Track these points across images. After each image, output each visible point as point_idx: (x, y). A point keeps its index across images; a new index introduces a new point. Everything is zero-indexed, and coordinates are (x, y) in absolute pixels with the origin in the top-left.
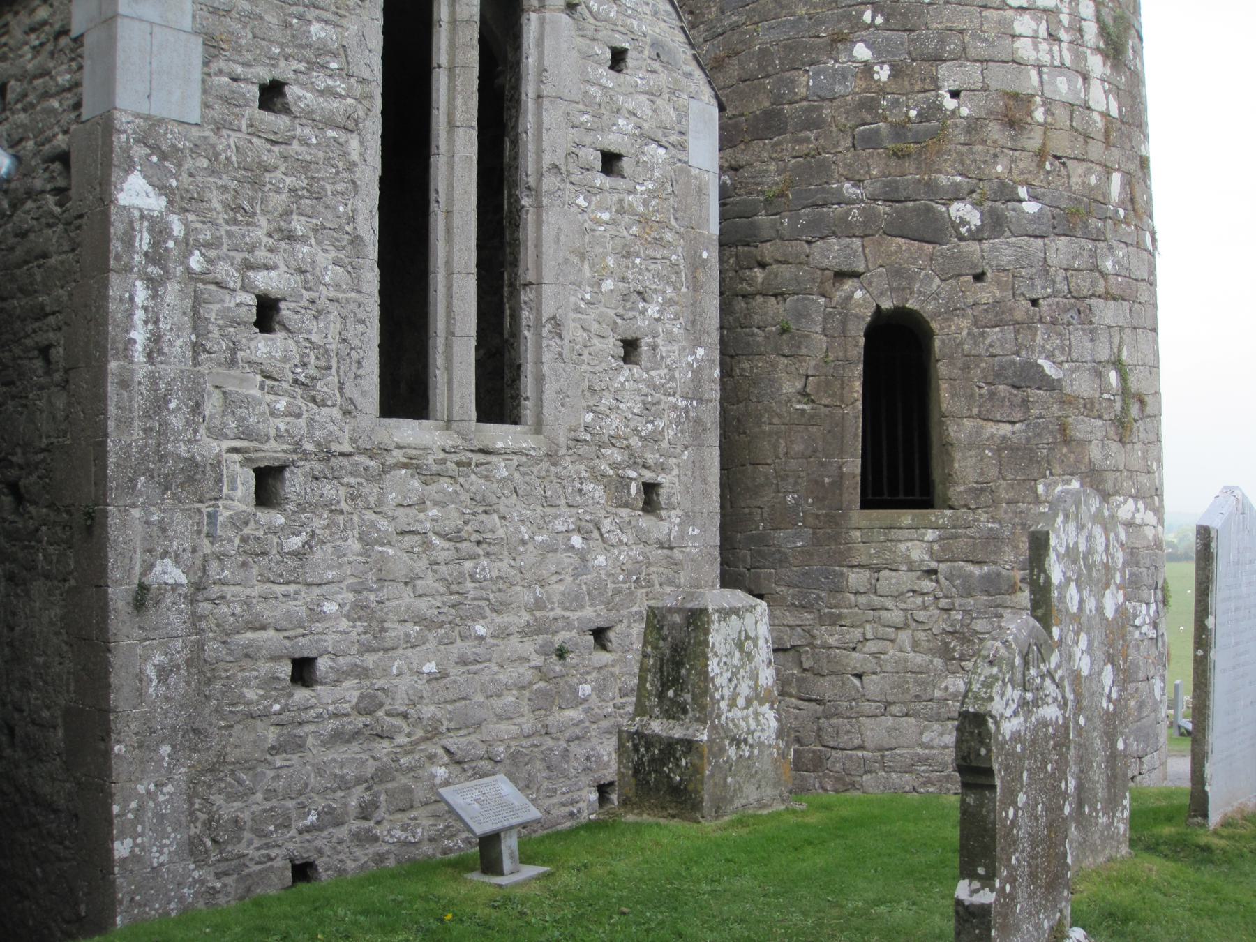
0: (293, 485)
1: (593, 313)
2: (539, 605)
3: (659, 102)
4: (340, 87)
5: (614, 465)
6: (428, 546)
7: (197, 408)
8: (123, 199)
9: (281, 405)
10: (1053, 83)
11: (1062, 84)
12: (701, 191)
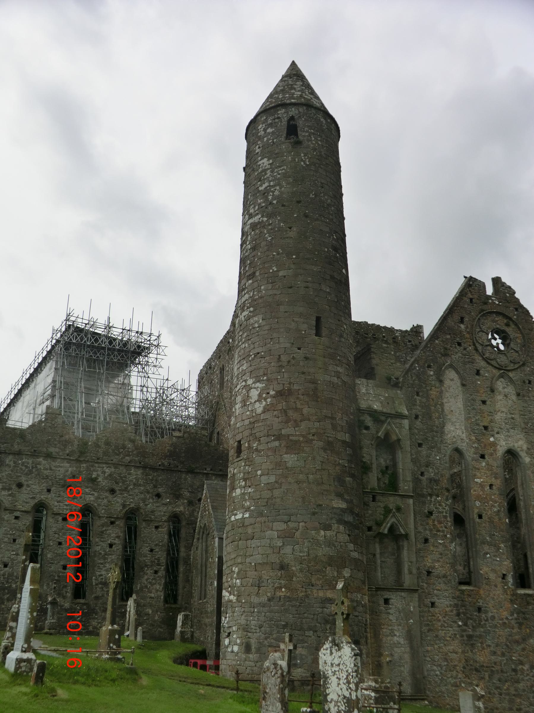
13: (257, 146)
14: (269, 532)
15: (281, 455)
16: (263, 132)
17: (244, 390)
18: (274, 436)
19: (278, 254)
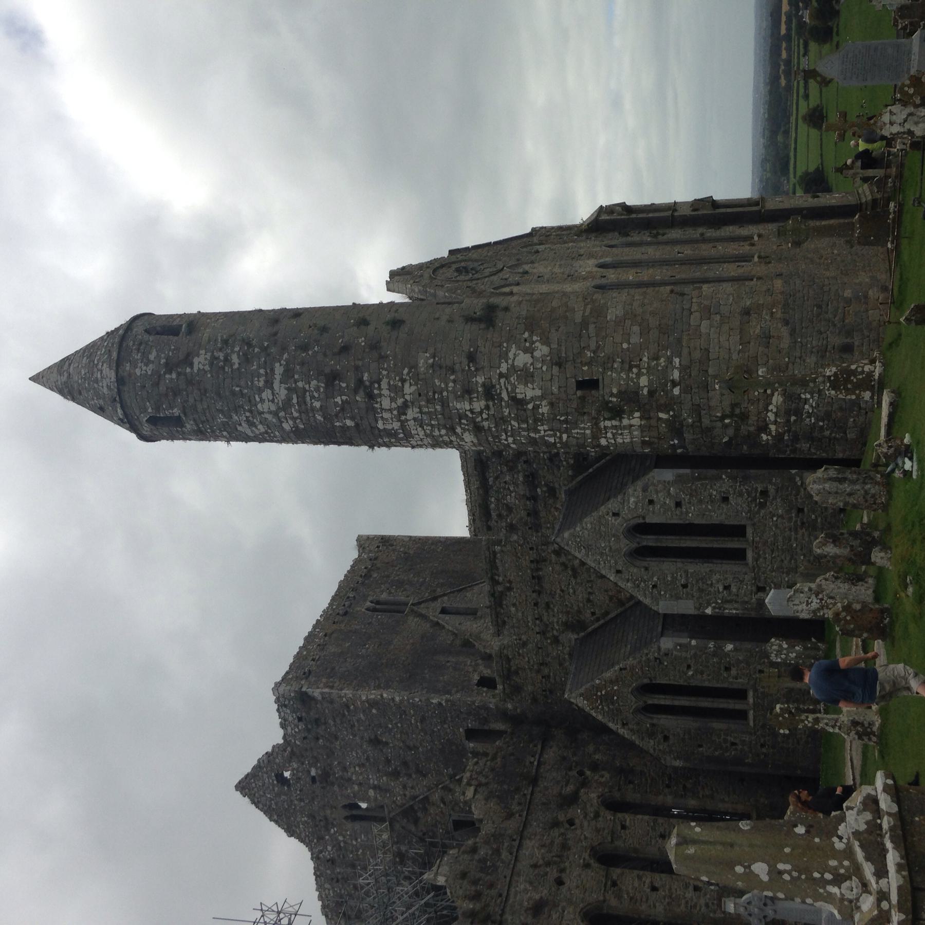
0: (761, 585)
2: (790, 530)
3: (659, 489)
4: (679, 574)
5: (756, 506)
6: (774, 557)
7: (747, 602)
8: (710, 613)
9: (745, 587)
11: (636, 433)
12: (679, 476)
15: (608, 322)
16: (151, 366)
17: (512, 379)
18: (581, 331)
19: (343, 337)
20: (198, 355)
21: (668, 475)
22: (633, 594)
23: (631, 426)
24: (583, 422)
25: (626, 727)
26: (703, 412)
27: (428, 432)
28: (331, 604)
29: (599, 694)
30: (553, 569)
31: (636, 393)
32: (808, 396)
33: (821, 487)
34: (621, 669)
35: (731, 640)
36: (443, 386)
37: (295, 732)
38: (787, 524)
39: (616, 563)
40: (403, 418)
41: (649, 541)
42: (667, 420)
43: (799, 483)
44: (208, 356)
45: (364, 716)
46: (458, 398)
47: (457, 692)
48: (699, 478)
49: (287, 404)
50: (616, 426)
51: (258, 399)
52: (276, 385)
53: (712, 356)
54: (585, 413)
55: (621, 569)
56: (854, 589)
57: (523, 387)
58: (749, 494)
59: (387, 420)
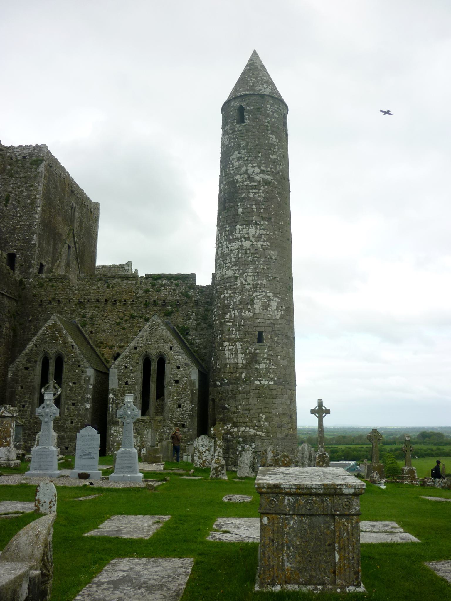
1: (172, 402)
4: (134, 381)
8: (109, 396)
10: (231, 361)
11: (232, 361)
12: (194, 382)
13: (267, 121)
14: (285, 396)
17: (264, 298)
20: (276, 138)
21: (195, 376)
22: (122, 355)
23: (237, 358)
24: (240, 334)
25: (34, 346)
26: (245, 395)
27: (234, 252)
28: (76, 184)
29: (57, 333)
30: (120, 312)
31: (256, 362)
32: (253, 447)
33: (306, 450)
34: (73, 346)
35: (93, 407)
36: (261, 262)
37: (16, 153)
38: (165, 437)
39: (141, 347)
40: (243, 240)
41: (154, 366)
42: (241, 377)
43: (189, 443)
44: (275, 143)
45: (26, 195)
46: (255, 270)
47: (39, 250)
48: (192, 393)
49: (251, 179)
50: (237, 351)
51: (254, 165)
52: (261, 175)
53: (274, 400)
54: (245, 335)
55: (137, 349)
56: (247, 467)
57: (260, 304)
58: (183, 418)
59: (242, 231)
